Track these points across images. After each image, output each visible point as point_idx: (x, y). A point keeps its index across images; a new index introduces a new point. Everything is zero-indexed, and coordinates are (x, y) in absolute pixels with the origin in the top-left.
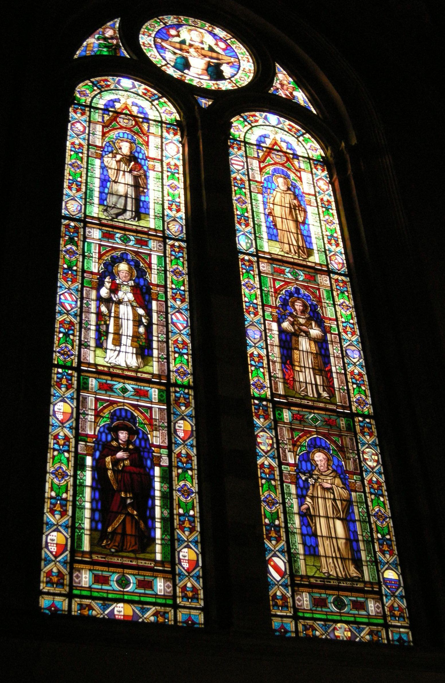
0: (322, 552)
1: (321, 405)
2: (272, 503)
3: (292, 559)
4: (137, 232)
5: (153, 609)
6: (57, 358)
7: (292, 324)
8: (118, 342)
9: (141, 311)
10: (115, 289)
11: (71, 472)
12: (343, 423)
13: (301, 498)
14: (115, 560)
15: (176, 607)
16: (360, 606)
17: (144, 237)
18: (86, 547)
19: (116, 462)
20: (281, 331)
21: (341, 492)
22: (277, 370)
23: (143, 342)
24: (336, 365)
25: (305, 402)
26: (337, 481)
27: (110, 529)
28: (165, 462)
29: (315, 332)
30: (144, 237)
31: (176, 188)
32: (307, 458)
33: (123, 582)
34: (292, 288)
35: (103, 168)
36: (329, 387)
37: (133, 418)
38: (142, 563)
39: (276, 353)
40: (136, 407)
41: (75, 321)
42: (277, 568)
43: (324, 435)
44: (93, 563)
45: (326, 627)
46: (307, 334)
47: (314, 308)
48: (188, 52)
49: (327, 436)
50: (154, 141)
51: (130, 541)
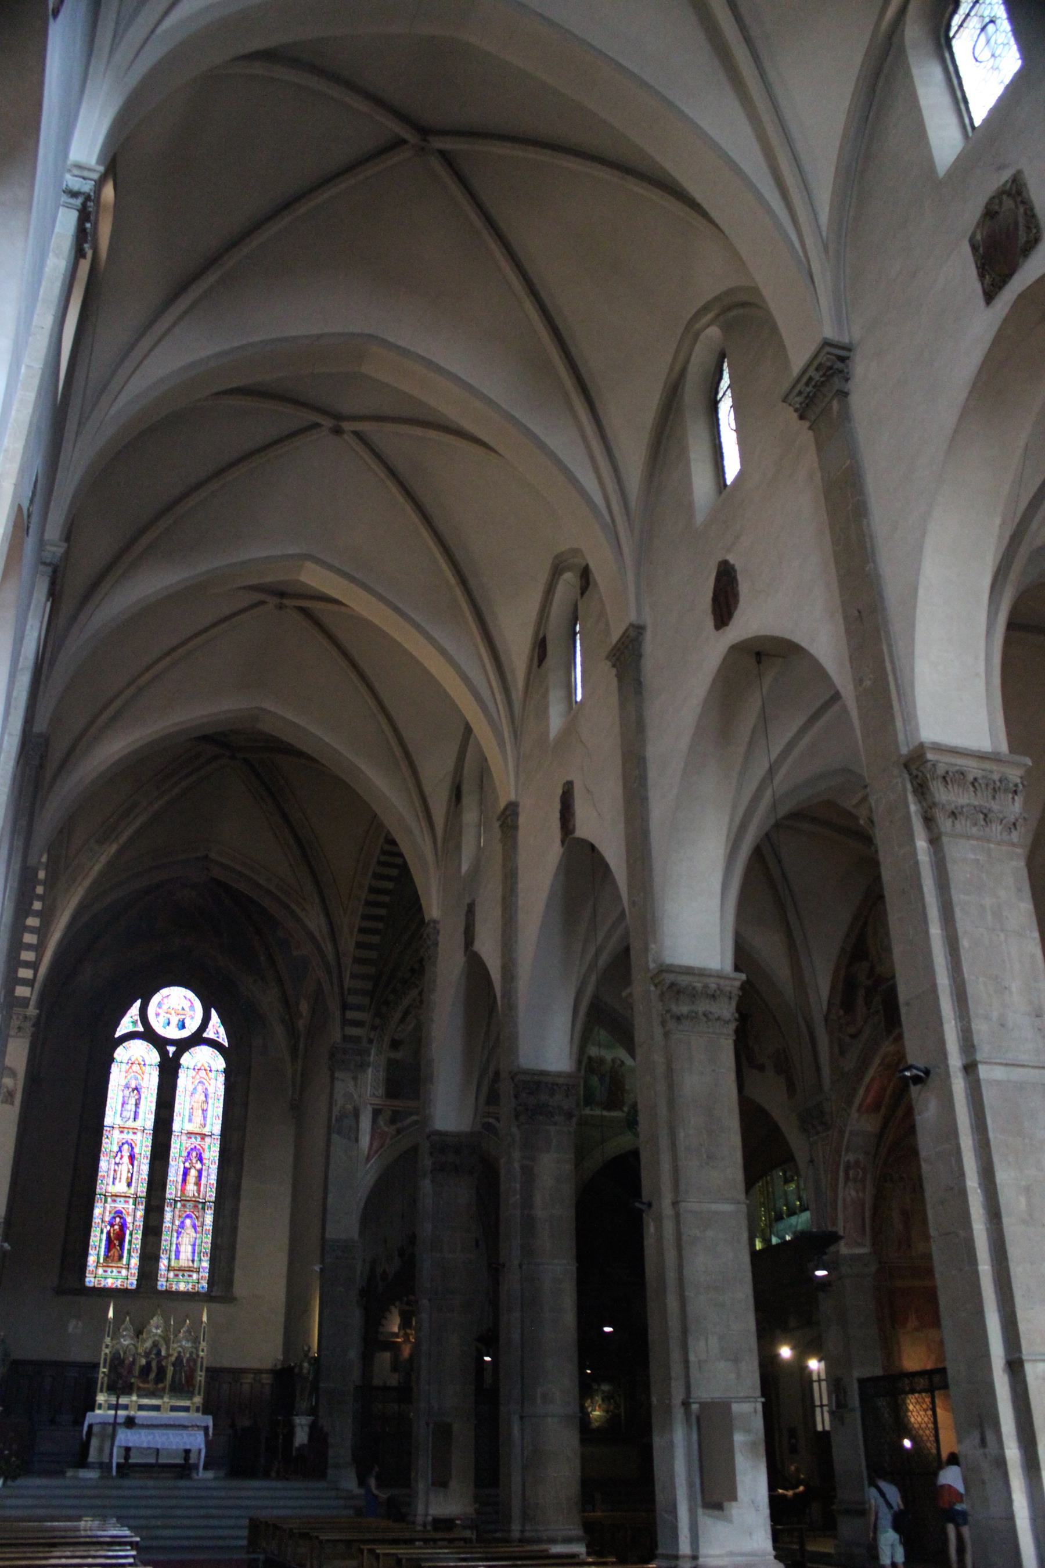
0: (181, 1257)
1: (194, 1199)
2: (166, 1240)
3: (169, 1260)
4: (133, 1129)
5: (120, 1280)
6: (98, 1191)
8: (120, 1181)
9: (130, 1167)
10: (122, 1157)
12: (200, 1206)
13: (178, 1238)
14: (111, 1265)
15: (127, 1279)
17: (136, 1131)
18: (101, 1261)
19: (114, 1230)
20: (184, 1168)
23: (129, 1180)
24: (203, 1181)
25: (188, 1199)
26: (193, 1230)
27: (110, 1254)
28: (131, 1229)
29: (199, 1166)
30: (136, 1131)
31: (151, 1102)
32: (183, 1223)
33: (112, 1272)
34: (193, 1146)
35: (124, 1097)
36: (199, 1191)
37: (121, 1213)
38: (119, 1265)
39: (180, 1179)
40: (123, 1208)
41: (106, 1174)
42: (164, 1264)
44: (103, 1266)
45: (177, 1284)
46: (195, 1167)
47: (201, 1154)
48: (171, 1014)
49: (193, 1212)
50: (146, 1076)
51: (116, 1258)
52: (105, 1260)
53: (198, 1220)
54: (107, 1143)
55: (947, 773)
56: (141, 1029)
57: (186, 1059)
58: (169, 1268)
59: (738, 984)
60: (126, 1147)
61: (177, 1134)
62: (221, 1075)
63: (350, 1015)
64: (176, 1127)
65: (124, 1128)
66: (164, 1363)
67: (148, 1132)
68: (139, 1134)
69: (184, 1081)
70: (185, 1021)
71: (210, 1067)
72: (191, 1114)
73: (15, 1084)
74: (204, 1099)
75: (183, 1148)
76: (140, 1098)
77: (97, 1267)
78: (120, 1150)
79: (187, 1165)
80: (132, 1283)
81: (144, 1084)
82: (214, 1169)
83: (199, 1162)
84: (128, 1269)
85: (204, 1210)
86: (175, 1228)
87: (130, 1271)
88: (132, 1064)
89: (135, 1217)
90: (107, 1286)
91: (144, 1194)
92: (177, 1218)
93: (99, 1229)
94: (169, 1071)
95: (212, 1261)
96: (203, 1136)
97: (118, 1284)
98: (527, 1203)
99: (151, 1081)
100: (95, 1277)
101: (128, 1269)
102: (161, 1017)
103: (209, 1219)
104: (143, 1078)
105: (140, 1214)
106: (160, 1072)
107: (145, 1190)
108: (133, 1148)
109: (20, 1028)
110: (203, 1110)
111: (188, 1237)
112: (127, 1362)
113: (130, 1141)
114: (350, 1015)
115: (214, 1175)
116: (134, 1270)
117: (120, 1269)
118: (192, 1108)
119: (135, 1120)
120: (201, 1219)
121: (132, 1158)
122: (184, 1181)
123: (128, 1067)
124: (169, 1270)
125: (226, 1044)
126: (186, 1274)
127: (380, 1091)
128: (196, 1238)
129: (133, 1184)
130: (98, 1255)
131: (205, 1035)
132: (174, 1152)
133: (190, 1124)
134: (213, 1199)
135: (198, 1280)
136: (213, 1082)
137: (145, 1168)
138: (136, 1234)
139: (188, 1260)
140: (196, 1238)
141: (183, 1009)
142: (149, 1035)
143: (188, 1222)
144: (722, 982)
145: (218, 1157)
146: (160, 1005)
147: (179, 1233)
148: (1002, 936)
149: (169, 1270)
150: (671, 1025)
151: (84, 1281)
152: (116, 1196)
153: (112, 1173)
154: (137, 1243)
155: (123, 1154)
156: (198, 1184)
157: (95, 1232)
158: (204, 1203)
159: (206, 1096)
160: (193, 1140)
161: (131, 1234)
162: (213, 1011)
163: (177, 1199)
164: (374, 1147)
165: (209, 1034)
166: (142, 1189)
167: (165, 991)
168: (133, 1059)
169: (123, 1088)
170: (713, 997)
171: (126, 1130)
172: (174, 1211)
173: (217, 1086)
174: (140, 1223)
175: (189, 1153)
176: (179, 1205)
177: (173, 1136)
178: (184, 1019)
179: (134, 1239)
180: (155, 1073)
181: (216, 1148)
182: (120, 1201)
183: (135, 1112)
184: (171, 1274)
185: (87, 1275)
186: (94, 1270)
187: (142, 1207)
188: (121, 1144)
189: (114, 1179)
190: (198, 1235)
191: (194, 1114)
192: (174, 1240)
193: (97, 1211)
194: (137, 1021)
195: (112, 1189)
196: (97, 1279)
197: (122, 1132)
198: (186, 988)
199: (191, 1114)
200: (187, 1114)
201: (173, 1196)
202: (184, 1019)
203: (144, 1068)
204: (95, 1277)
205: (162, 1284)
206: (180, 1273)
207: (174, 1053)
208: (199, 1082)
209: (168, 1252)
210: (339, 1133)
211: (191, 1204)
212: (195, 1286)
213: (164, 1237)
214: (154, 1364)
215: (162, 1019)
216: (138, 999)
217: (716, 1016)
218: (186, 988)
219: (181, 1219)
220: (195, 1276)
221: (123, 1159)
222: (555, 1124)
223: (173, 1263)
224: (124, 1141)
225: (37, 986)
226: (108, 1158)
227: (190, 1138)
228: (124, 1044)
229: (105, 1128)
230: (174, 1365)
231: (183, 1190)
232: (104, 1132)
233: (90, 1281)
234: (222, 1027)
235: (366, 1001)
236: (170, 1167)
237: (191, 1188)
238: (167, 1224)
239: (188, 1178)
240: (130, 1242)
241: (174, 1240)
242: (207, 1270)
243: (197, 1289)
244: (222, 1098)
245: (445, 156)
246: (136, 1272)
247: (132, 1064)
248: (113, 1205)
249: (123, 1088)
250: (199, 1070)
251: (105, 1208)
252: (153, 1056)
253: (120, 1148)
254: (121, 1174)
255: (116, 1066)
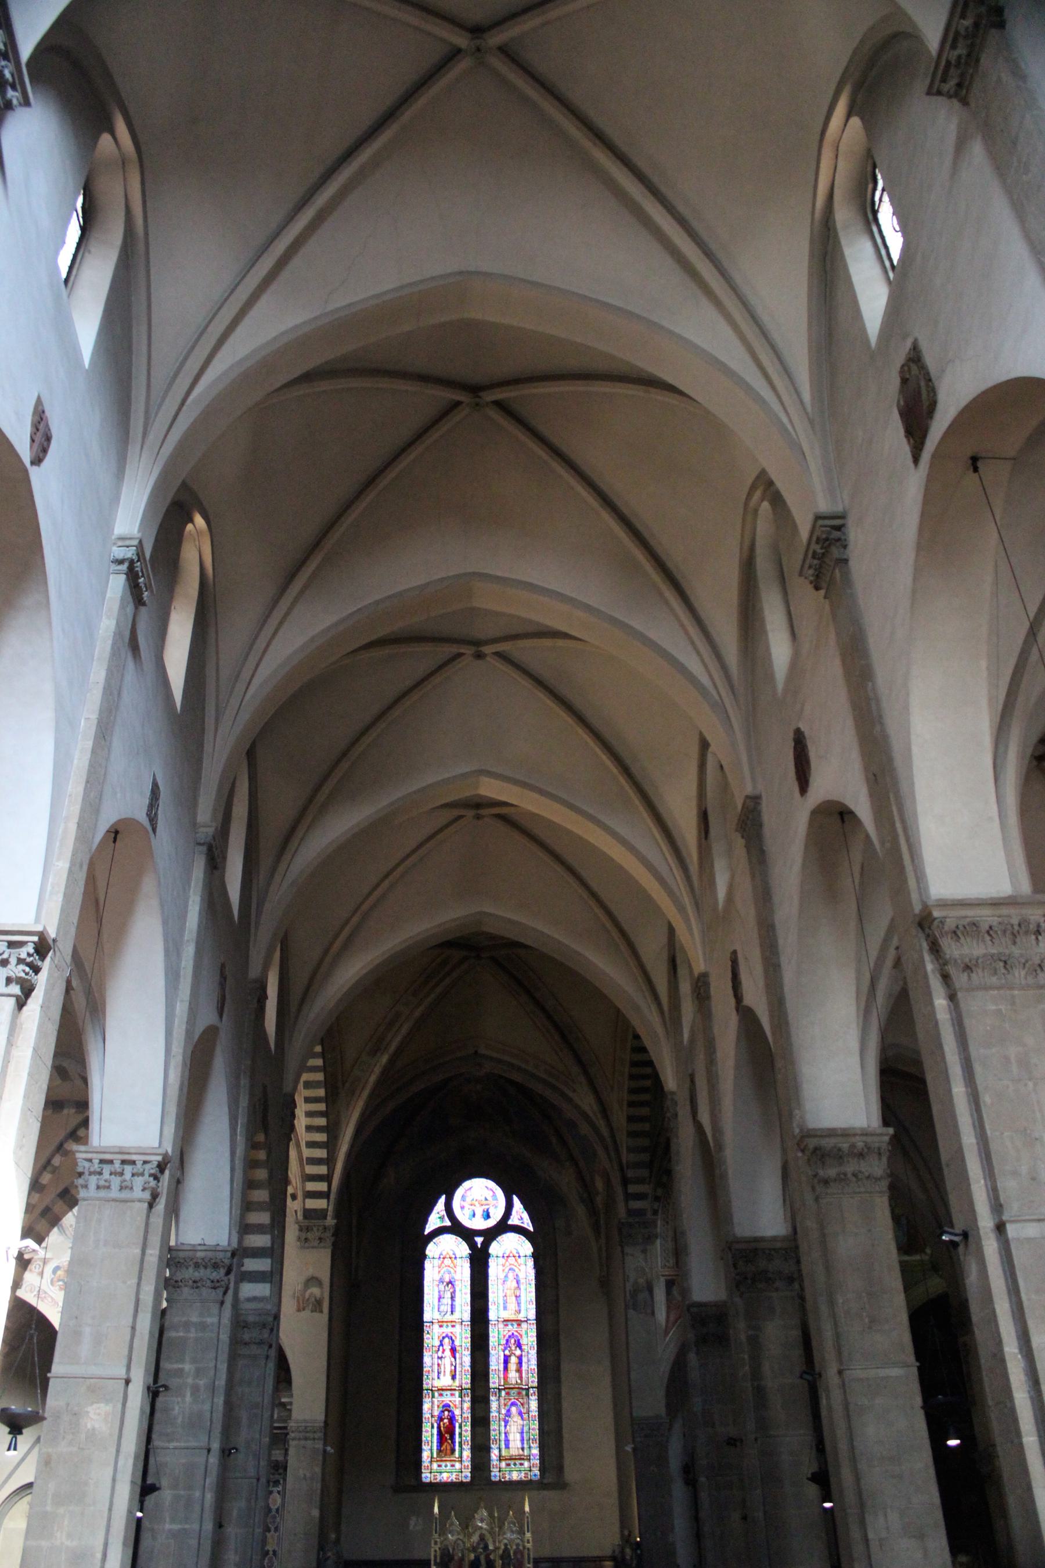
0: (510, 1446)
1: (517, 1386)
2: (494, 1430)
4: (452, 1322)
5: (455, 1474)
6: (425, 1386)
7: (509, 1351)
8: (444, 1375)
9: (453, 1360)
10: (443, 1352)
11: (430, 1430)
12: (524, 1392)
13: (505, 1426)
14: (444, 1459)
15: (461, 1472)
16: (521, 1464)
17: (453, 1324)
18: (435, 1456)
19: (444, 1424)
20: (505, 1355)
21: (520, 1422)
22: (502, 1376)
23: (453, 1373)
24: (524, 1367)
26: (520, 1418)
28: (460, 1421)
29: (518, 1352)
30: (453, 1324)
31: (466, 1294)
32: (509, 1411)
33: (446, 1466)
34: (510, 1333)
35: (439, 1292)
36: (521, 1378)
37: (449, 1406)
38: (452, 1459)
40: (450, 1401)
41: (430, 1370)
42: (495, 1455)
43: (517, 1399)
44: (437, 1461)
45: (509, 1474)
46: (514, 1354)
47: (519, 1340)
50: (458, 1269)
51: (448, 1451)
52: (438, 1454)
53: (523, 1408)
54: (428, 1339)
55: (957, 927)
56: (448, 1223)
57: (494, 1248)
58: (501, 1458)
59: (887, 1139)
60: (446, 1340)
61: (493, 1323)
62: (530, 1260)
63: (632, 1189)
64: (492, 1315)
65: (443, 1322)
66: (492, 1557)
67: (466, 1323)
68: (458, 1326)
69: (495, 1270)
70: (490, 1211)
71: (519, 1253)
72: (505, 1302)
73: (322, 1293)
74: (516, 1285)
75: (501, 1336)
76: (454, 1292)
77: (431, 1462)
78: (442, 1344)
79: (507, 1352)
80: (466, 1475)
81: (457, 1277)
82: (533, 1354)
83: (518, 1348)
84: (461, 1461)
85: (528, 1396)
86: (502, 1416)
87: (463, 1464)
88: (444, 1258)
89: (463, 1409)
90: (443, 1481)
91: (469, 1386)
92: (502, 1407)
93: (430, 1424)
94: (479, 1261)
95: (542, 1448)
96: (519, 1322)
97: (453, 1478)
98: (756, 1374)
99: (463, 1273)
100: (431, 1473)
101: (461, 1461)
102: (466, 1209)
103: (534, 1405)
104: (455, 1271)
105: (467, 1405)
106: (471, 1264)
107: (469, 1381)
108: (453, 1341)
109: (320, 1239)
110: (516, 1297)
111: (515, 1425)
112: (456, 1558)
113: (450, 1334)
114: (632, 1189)
115: (534, 1360)
116: (467, 1463)
117: (453, 1463)
118: (505, 1296)
119: (452, 1313)
120: (526, 1406)
121: (453, 1350)
122: (506, 1368)
123: (440, 1262)
124: (500, 1460)
125: (531, 1229)
126: (518, 1462)
127: (671, 1262)
128: (523, 1426)
129: (458, 1376)
130: (431, 1450)
131: (510, 1222)
132: (493, 1341)
133: (506, 1311)
134: (536, 1384)
135: (530, 1467)
136: (523, 1267)
137: (467, 1360)
138: (465, 1426)
139: (518, 1448)
140: (523, 1426)
141: (486, 1199)
142: (456, 1228)
143: (514, 1409)
144: (869, 1139)
145: (536, 1342)
146: (463, 1198)
147: (506, 1422)
148: (1030, 1084)
149: (500, 1460)
150: (819, 1189)
151: (421, 1478)
152: (442, 1390)
153: (436, 1367)
154: (467, 1435)
155: (445, 1347)
156: (519, 1370)
157: (426, 1427)
158: (528, 1389)
159: (518, 1282)
160: (510, 1327)
161: (460, 1427)
162: (516, 1200)
163: (500, 1387)
164: (672, 1318)
165: (513, 1221)
166: (466, 1380)
167: (467, 1184)
168: (444, 1253)
169: (437, 1283)
170: (861, 1155)
171: (445, 1324)
172: (499, 1400)
173: (527, 1271)
174: (468, 1414)
175: (507, 1341)
176: (503, 1393)
177: (490, 1326)
178: (488, 1210)
179: (464, 1432)
180: (467, 1266)
181: (533, 1333)
182: (447, 1395)
183: (452, 1305)
184: (503, 1464)
185: (423, 1471)
186: (429, 1465)
187: (468, 1399)
188: (441, 1338)
189: (439, 1373)
190: (525, 1422)
191: (508, 1301)
192: (502, 1428)
193: (426, 1406)
194: (444, 1216)
195: (438, 1384)
196: (433, 1474)
197: (441, 1326)
198: (487, 1178)
199: (505, 1302)
200: (501, 1302)
201: (497, 1385)
202: (488, 1210)
203: (455, 1261)
204: (431, 1473)
205: (495, 1475)
206: (512, 1462)
207: (482, 1244)
208: (510, 1269)
209: (498, 1441)
210: (634, 1309)
211: (515, 1391)
212: (527, 1474)
213: (492, 1428)
214: (482, 1558)
215: (468, 1212)
216: (442, 1195)
217: (867, 1174)
218: (487, 1178)
219: (507, 1408)
220: (526, 1464)
221: (445, 1353)
222: (777, 1290)
223: (504, 1453)
224: (444, 1335)
225: (333, 1196)
226: (431, 1353)
227: (507, 1325)
228: (434, 1241)
229: (425, 1324)
230: (502, 1557)
231: (506, 1378)
232: (425, 1328)
233: (426, 1477)
234: (525, 1212)
235: (644, 1173)
236: (491, 1355)
237: (513, 1375)
238: (494, 1414)
239: (509, 1365)
240: (460, 1434)
241: (502, 1428)
242: (538, 1457)
243: (529, 1477)
244: (533, 1282)
245: (499, 404)
246: (469, 1464)
247: (444, 1258)
248: (440, 1399)
249: (437, 1283)
250: (507, 1257)
251: (433, 1403)
252: (464, 1249)
253: (441, 1341)
254: (445, 1368)
255: (429, 1262)
